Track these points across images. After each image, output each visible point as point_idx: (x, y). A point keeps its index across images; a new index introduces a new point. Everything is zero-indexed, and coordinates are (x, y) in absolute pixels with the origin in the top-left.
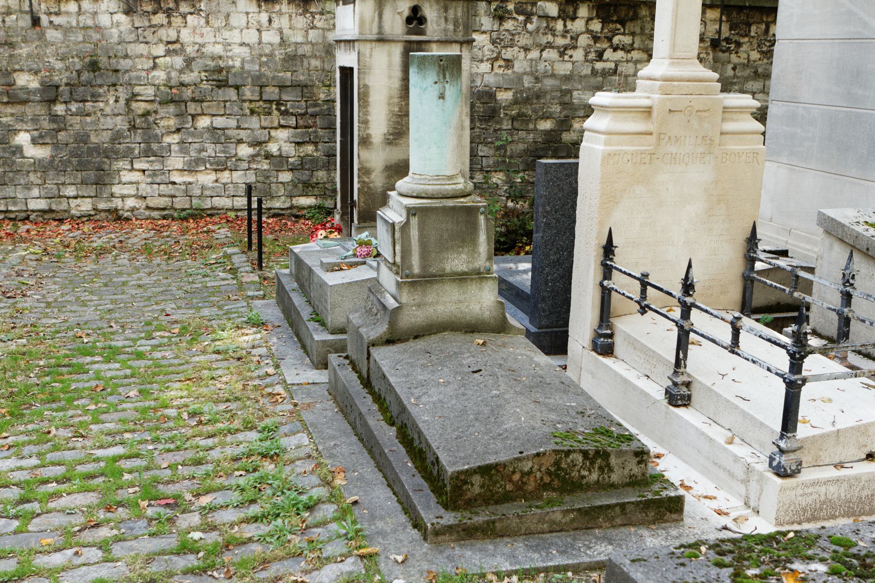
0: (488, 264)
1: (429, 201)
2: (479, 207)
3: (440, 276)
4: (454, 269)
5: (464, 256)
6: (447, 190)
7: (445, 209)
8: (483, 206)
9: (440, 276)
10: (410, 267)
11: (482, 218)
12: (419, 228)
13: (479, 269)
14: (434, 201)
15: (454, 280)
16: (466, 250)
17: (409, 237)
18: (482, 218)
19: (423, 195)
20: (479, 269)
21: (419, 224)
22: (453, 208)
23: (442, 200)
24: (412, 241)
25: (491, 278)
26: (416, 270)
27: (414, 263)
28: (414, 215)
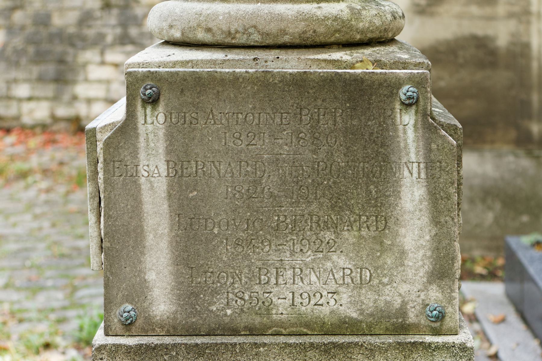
0: (434, 294)
1: (218, 55)
2: (398, 84)
3: (252, 331)
4: (307, 309)
5: (342, 261)
6: (281, 18)
7: (267, 86)
8: (411, 79)
9: (252, 331)
10: (139, 292)
11: (407, 121)
12: (169, 151)
13: (402, 312)
14: (233, 55)
15: (303, 348)
16: (349, 236)
17: (133, 179)
18: (407, 121)
19: (201, 36)
20: (402, 312)
21: (170, 137)
22: (299, 83)
23: (261, 54)
24: (146, 197)
25: (446, 347)
26: (162, 304)
27: (151, 276)
28: (153, 101)
